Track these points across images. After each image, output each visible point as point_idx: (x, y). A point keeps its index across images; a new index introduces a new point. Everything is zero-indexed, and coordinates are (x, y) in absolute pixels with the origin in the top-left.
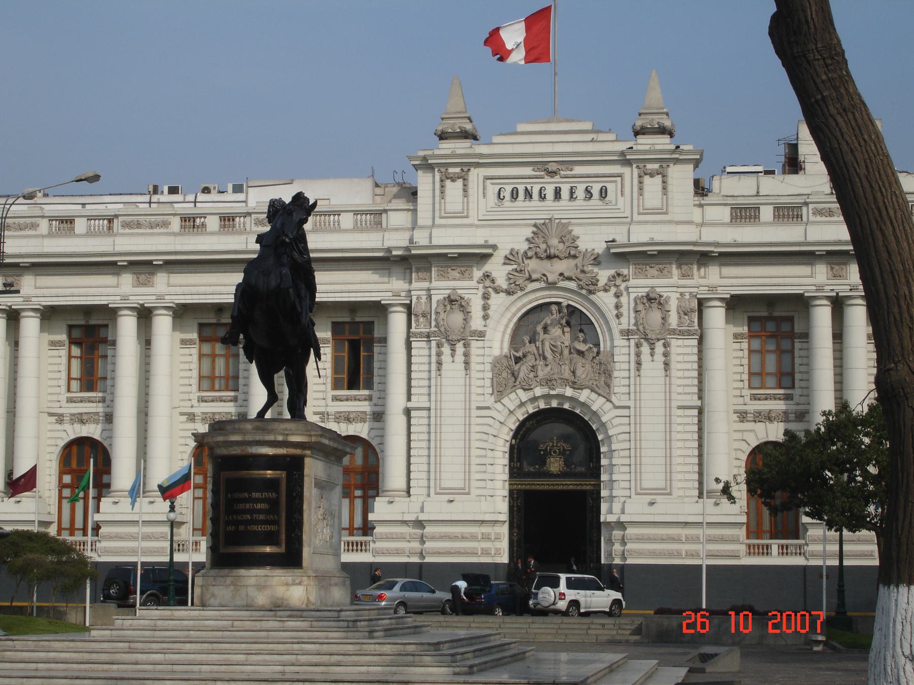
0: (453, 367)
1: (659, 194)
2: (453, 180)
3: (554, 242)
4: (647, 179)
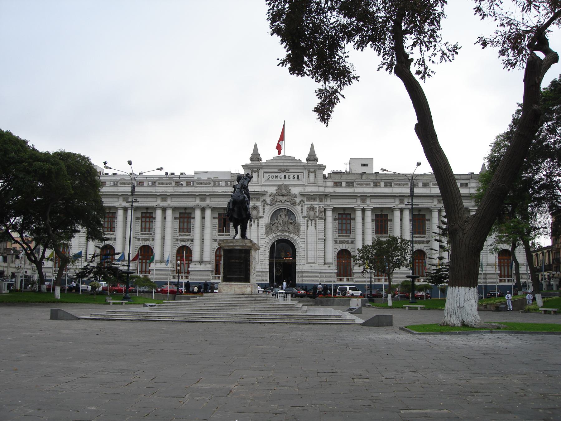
3: (284, 191)
4: (310, 174)
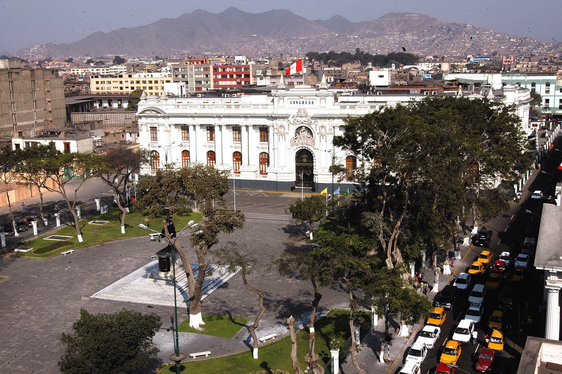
3: (302, 113)
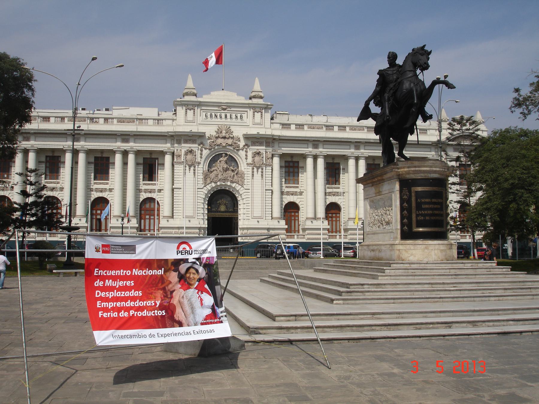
0: (190, 174)
1: (260, 118)
2: (190, 110)
